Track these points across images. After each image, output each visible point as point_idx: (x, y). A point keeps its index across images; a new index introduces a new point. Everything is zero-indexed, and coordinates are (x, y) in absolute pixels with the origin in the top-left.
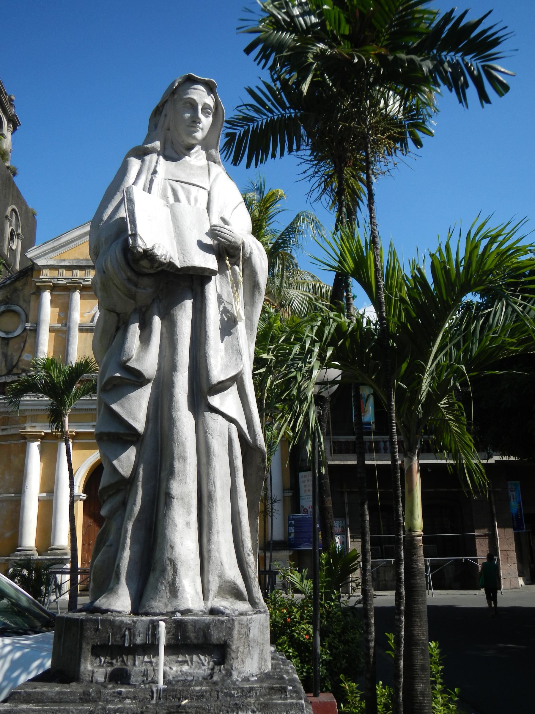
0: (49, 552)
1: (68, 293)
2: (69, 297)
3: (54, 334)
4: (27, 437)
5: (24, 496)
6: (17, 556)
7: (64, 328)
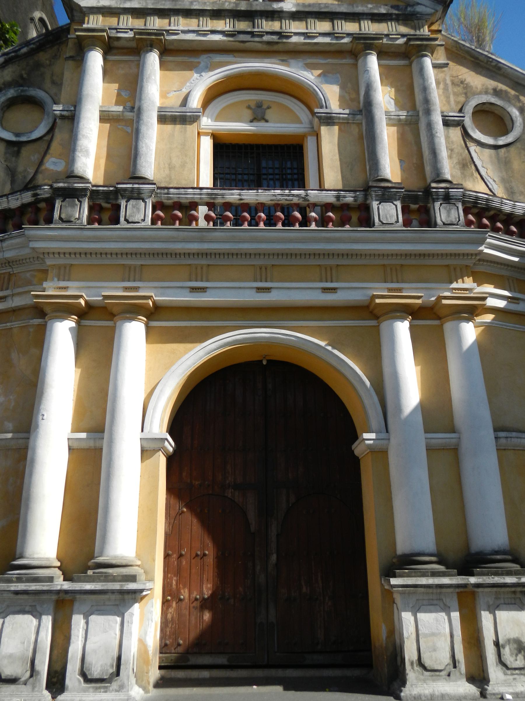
0: (90, 572)
1: (136, 58)
2: (138, 65)
3: (108, 125)
4: (47, 309)
5: (36, 437)
6: (9, 581)
7: (129, 115)
